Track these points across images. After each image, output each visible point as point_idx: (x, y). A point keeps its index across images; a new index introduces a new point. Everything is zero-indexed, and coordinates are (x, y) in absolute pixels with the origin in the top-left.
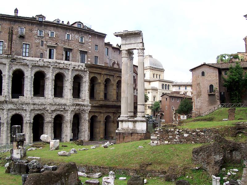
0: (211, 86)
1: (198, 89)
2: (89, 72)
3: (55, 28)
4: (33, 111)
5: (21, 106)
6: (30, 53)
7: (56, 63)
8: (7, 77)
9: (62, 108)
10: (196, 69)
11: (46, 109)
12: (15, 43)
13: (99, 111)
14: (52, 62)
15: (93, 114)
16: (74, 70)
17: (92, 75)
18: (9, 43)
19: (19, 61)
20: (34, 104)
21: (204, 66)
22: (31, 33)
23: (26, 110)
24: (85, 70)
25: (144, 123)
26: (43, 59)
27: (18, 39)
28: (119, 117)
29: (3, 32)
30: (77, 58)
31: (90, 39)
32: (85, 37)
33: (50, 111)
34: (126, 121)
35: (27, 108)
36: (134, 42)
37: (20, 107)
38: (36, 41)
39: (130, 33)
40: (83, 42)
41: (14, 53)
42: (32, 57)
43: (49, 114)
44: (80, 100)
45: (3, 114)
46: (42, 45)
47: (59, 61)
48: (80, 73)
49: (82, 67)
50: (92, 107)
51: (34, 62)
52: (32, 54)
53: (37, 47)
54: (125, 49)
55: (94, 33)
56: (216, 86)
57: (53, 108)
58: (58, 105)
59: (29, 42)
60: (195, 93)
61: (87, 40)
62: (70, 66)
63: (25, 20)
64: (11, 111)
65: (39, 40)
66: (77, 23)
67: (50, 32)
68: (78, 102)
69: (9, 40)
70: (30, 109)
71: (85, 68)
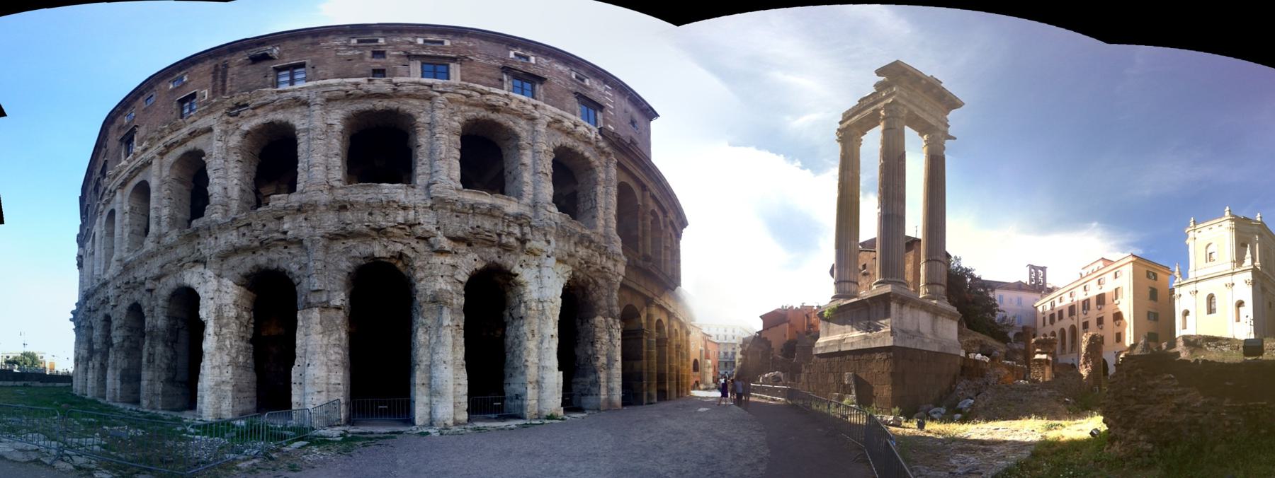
4: (339, 246)
23: (299, 242)
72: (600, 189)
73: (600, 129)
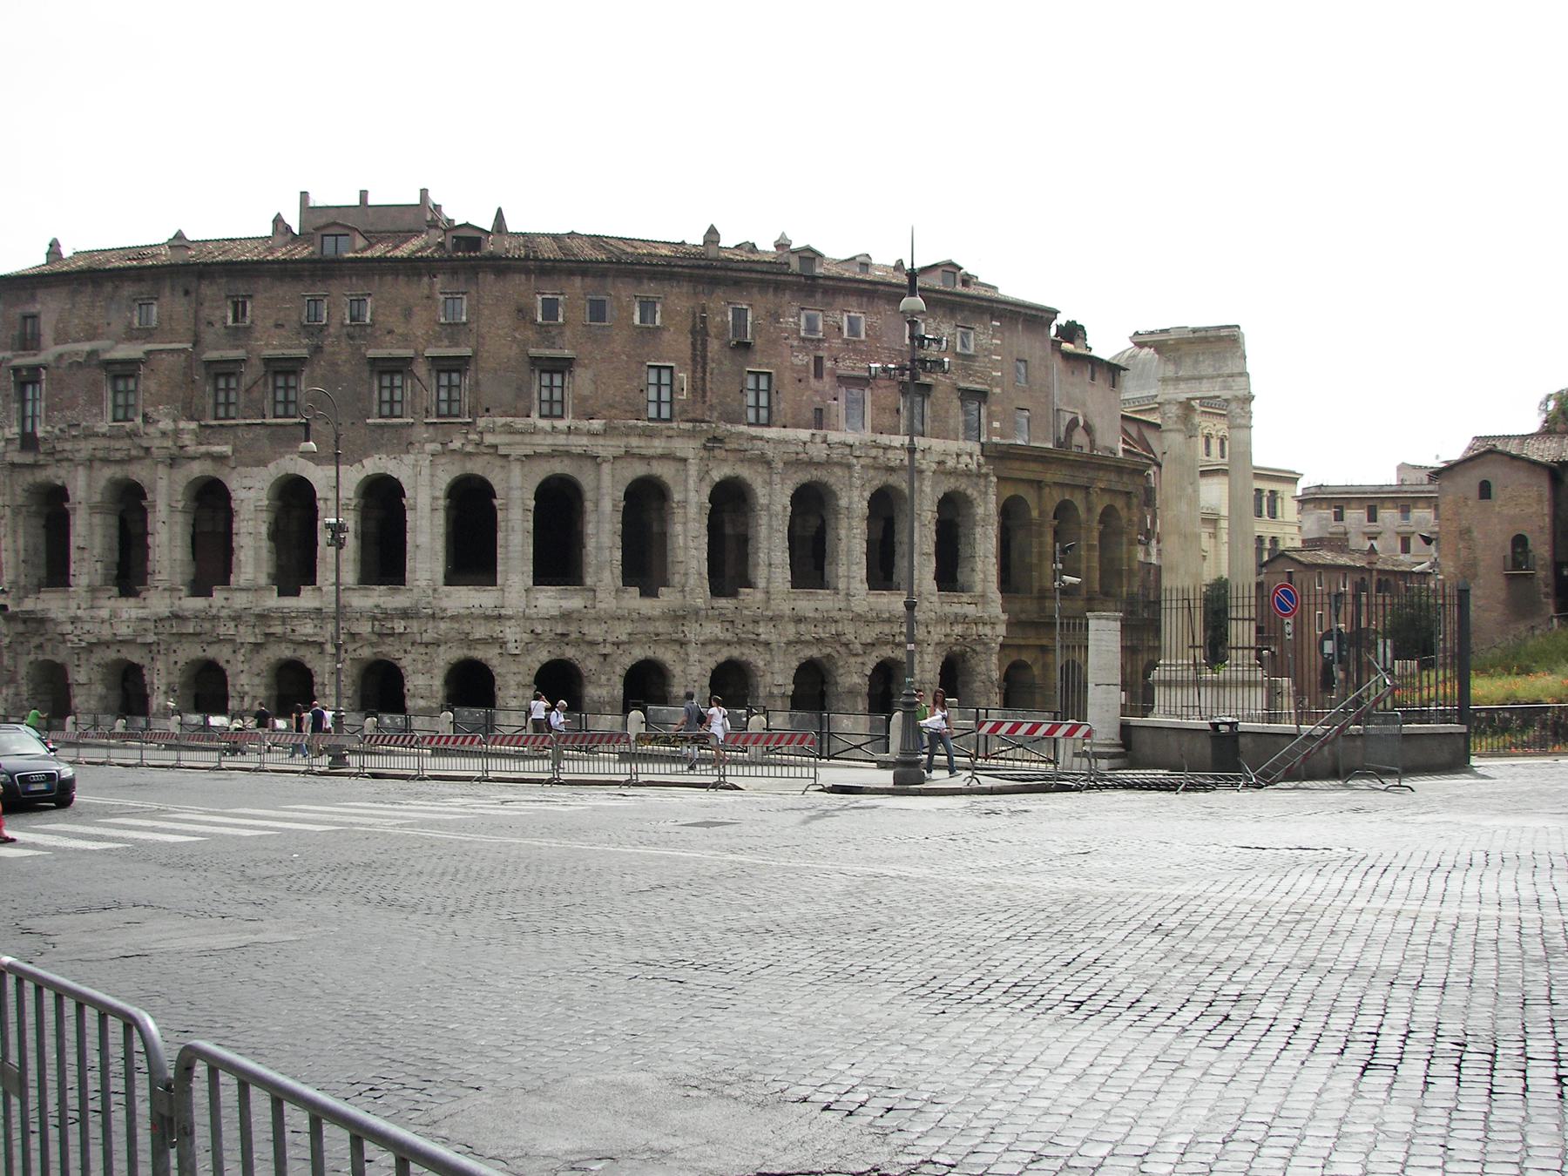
0: (1520, 541)
1: (1463, 553)
2: (994, 479)
3: (865, 299)
4: (792, 650)
5: (750, 627)
6: (774, 409)
7: (874, 447)
8: (692, 511)
9: (901, 633)
10: (1456, 469)
11: (844, 639)
12: (716, 371)
13: (1038, 643)
14: (857, 443)
15: (1014, 656)
16: (942, 470)
17: (1009, 491)
18: (694, 372)
19: (737, 446)
20: (799, 620)
21: (1489, 456)
22: (775, 328)
23: (767, 644)
24: (984, 470)
26: (823, 432)
27: (729, 353)
28: (1153, 665)
29: (672, 329)
30: (952, 422)
31: (998, 335)
32: (979, 328)
33: (858, 648)
34: (1181, 684)
35: (773, 638)
36: (1210, 371)
37: (748, 632)
38: (796, 361)
40: (971, 351)
41: (716, 414)
42: (785, 427)
43: (852, 660)
44: (965, 598)
45: (685, 661)
46: (818, 374)
47: (884, 439)
48: (963, 485)
49: (969, 461)
50: (1009, 624)
51: (792, 448)
52: (783, 413)
53: (802, 385)
54: (1175, 396)
55: (1013, 308)
56: (1541, 549)
57: (869, 634)
58: (889, 621)
59: (767, 366)
60: (1452, 569)
61: (984, 340)
62: (928, 457)
63: (754, 275)
64: (711, 648)
65: (807, 355)
66: (940, 270)
67: (845, 319)
68: (956, 609)
69: (694, 359)
70: (785, 640)
71: (982, 460)
72: (979, 530)
73: (982, 444)
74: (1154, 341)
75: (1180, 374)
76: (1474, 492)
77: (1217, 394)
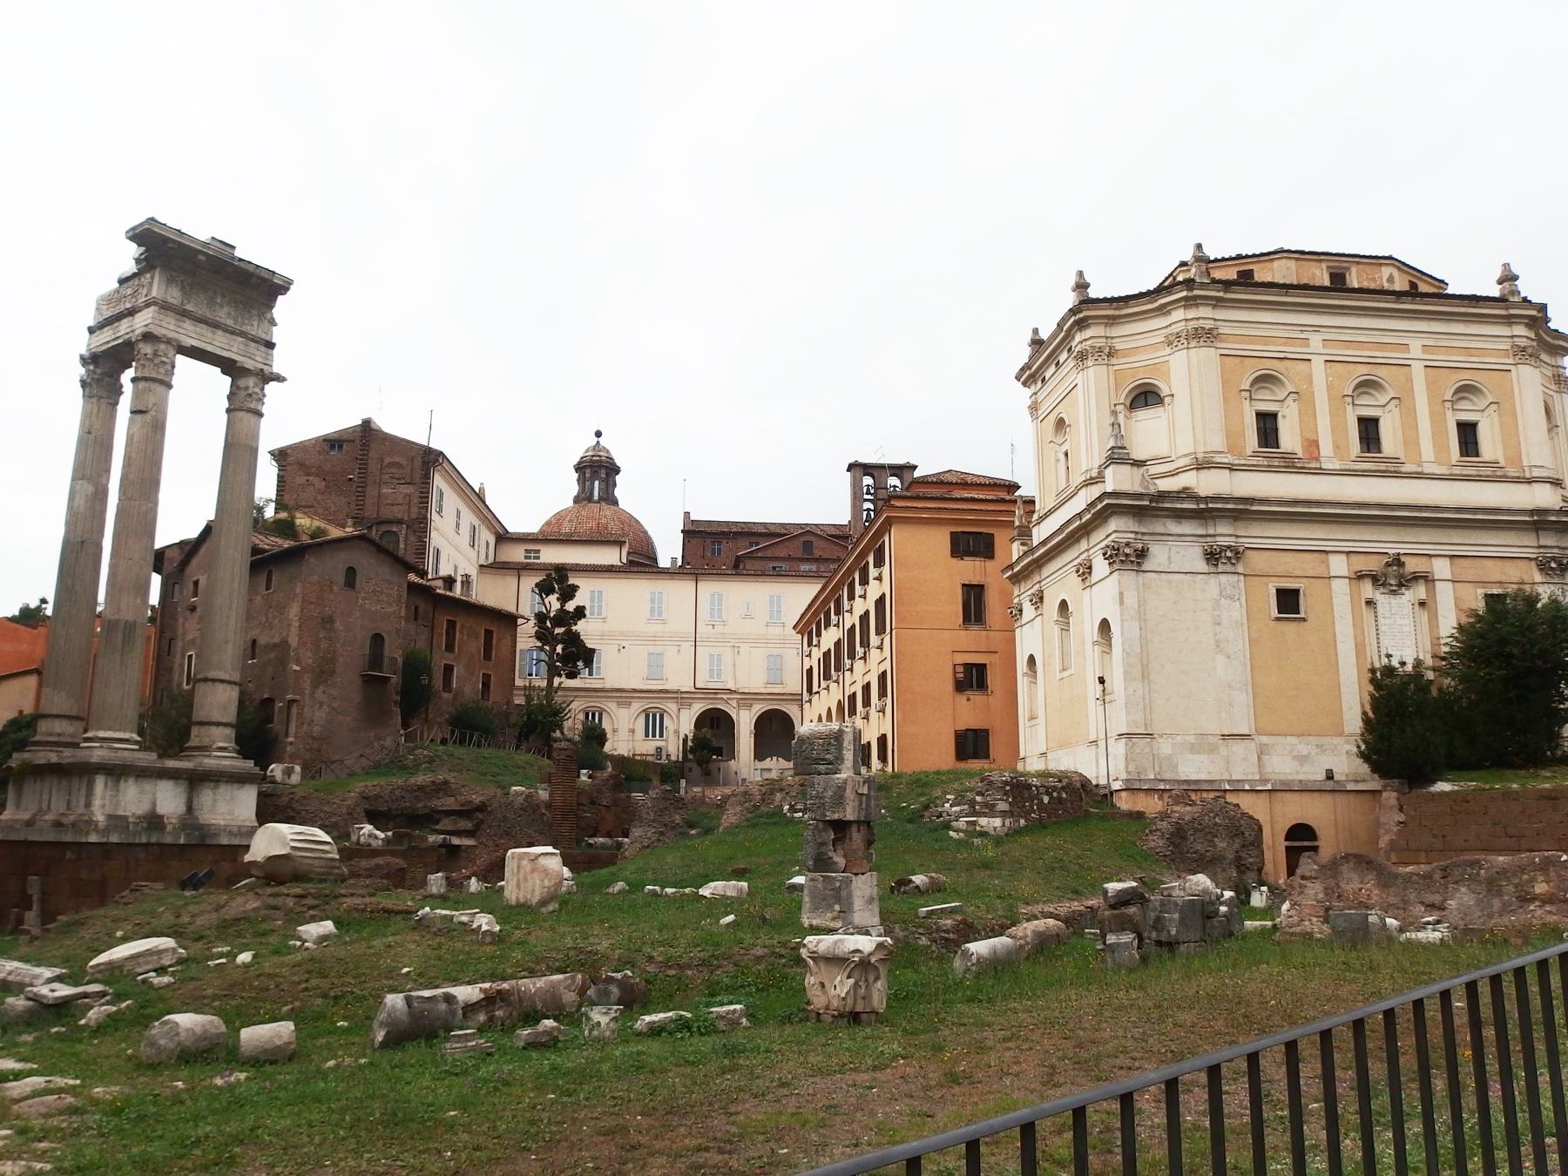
0: (378, 640)
1: (324, 645)
25: (247, 787)
36: (230, 322)
39: (242, 264)
54: (171, 335)
74: (180, 243)
75: (189, 307)
76: (341, 578)
77: (234, 357)
